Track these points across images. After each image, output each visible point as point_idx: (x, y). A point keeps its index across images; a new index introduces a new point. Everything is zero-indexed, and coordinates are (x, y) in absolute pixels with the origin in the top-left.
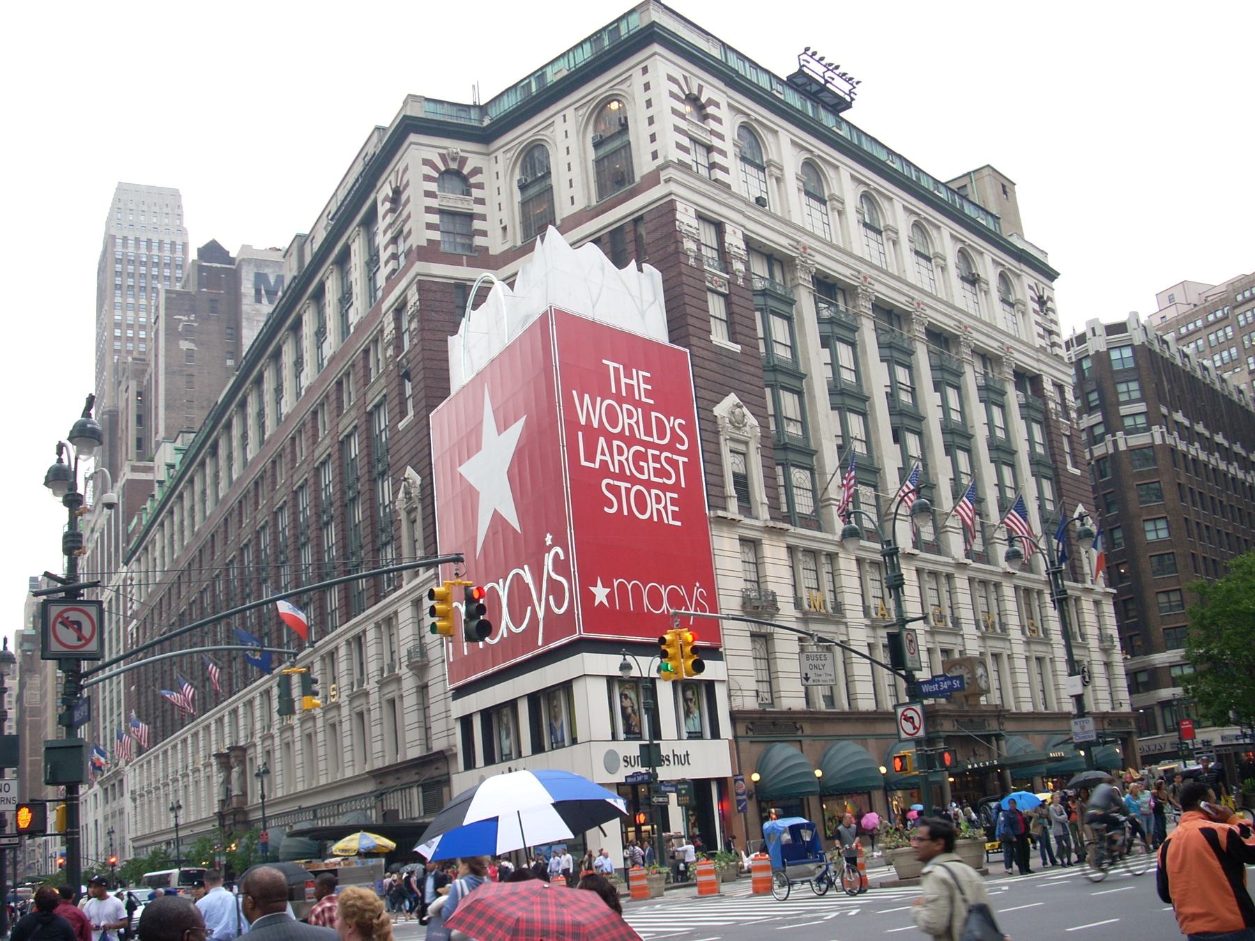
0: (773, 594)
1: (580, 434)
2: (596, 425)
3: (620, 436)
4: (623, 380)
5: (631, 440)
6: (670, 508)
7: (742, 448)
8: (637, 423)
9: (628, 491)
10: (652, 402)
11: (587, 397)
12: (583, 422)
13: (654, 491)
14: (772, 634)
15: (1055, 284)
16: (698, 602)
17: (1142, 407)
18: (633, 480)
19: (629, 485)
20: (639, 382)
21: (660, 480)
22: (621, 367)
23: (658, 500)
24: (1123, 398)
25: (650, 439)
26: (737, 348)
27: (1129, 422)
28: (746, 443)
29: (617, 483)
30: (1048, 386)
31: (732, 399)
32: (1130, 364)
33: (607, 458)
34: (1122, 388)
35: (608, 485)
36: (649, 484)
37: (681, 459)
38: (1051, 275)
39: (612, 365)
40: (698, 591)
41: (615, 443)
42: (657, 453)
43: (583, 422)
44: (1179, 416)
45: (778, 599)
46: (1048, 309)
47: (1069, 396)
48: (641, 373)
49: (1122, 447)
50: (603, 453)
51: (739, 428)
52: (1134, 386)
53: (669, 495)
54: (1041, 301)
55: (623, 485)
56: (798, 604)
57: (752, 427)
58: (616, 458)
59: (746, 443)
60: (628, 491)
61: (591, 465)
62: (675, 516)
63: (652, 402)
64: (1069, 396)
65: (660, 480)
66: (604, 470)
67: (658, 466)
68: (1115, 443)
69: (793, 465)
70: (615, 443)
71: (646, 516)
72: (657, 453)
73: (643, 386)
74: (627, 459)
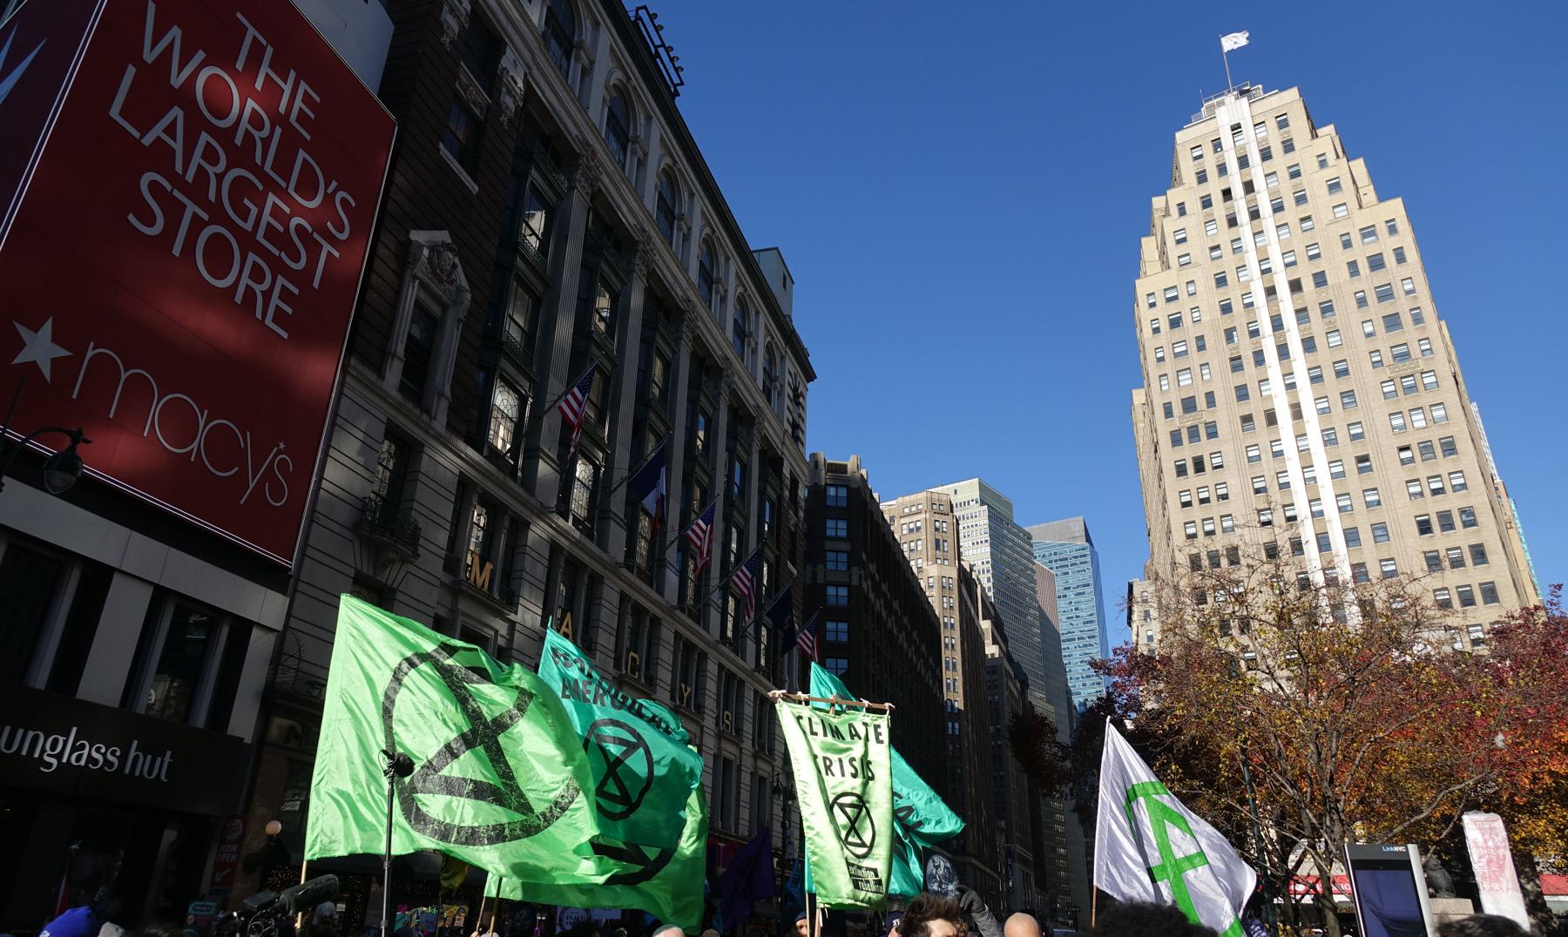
0: (417, 528)
1: (131, 71)
2: (177, 81)
3: (226, 136)
4: (265, 69)
5: (241, 155)
6: (275, 300)
7: (435, 309)
8: (266, 142)
9: (197, 225)
10: (308, 137)
11: (176, 32)
12: (149, 56)
13: (252, 257)
14: (395, 590)
15: (809, 385)
16: (269, 475)
17: (846, 546)
18: (218, 215)
19: (206, 217)
20: (294, 96)
21: (276, 252)
22: (270, 50)
23: (257, 275)
24: (830, 533)
25: (284, 185)
26: (475, 188)
27: (831, 556)
28: (445, 307)
29: (176, 193)
30: (786, 472)
31: (443, 236)
32: (843, 503)
33: (178, 146)
34: (830, 523)
35: (153, 186)
36: (248, 242)
37: (327, 247)
38: (810, 376)
39: (252, 32)
40: (278, 455)
41: (205, 137)
42: (287, 210)
43: (149, 56)
44: (872, 568)
45: (422, 541)
46: (798, 404)
47: (803, 493)
48: (303, 86)
49: (820, 580)
50: (171, 130)
51: (441, 280)
52: (842, 525)
53: (281, 280)
54: (797, 397)
55: (191, 208)
56: (452, 563)
57: (460, 290)
58: (197, 159)
59: (445, 307)
60: (197, 225)
61: (137, 134)
62: (279, 317)
63: (308, 137)
64: (803, 493)
65: (276, 252)
66: (160, 156)
67: (281, 229)
68: (814, 574)
69: (503, 379)
70: (205, 137)
71: (222, 284)
72: (287, 210)
73: (298, 103)
74: (220, 177)
